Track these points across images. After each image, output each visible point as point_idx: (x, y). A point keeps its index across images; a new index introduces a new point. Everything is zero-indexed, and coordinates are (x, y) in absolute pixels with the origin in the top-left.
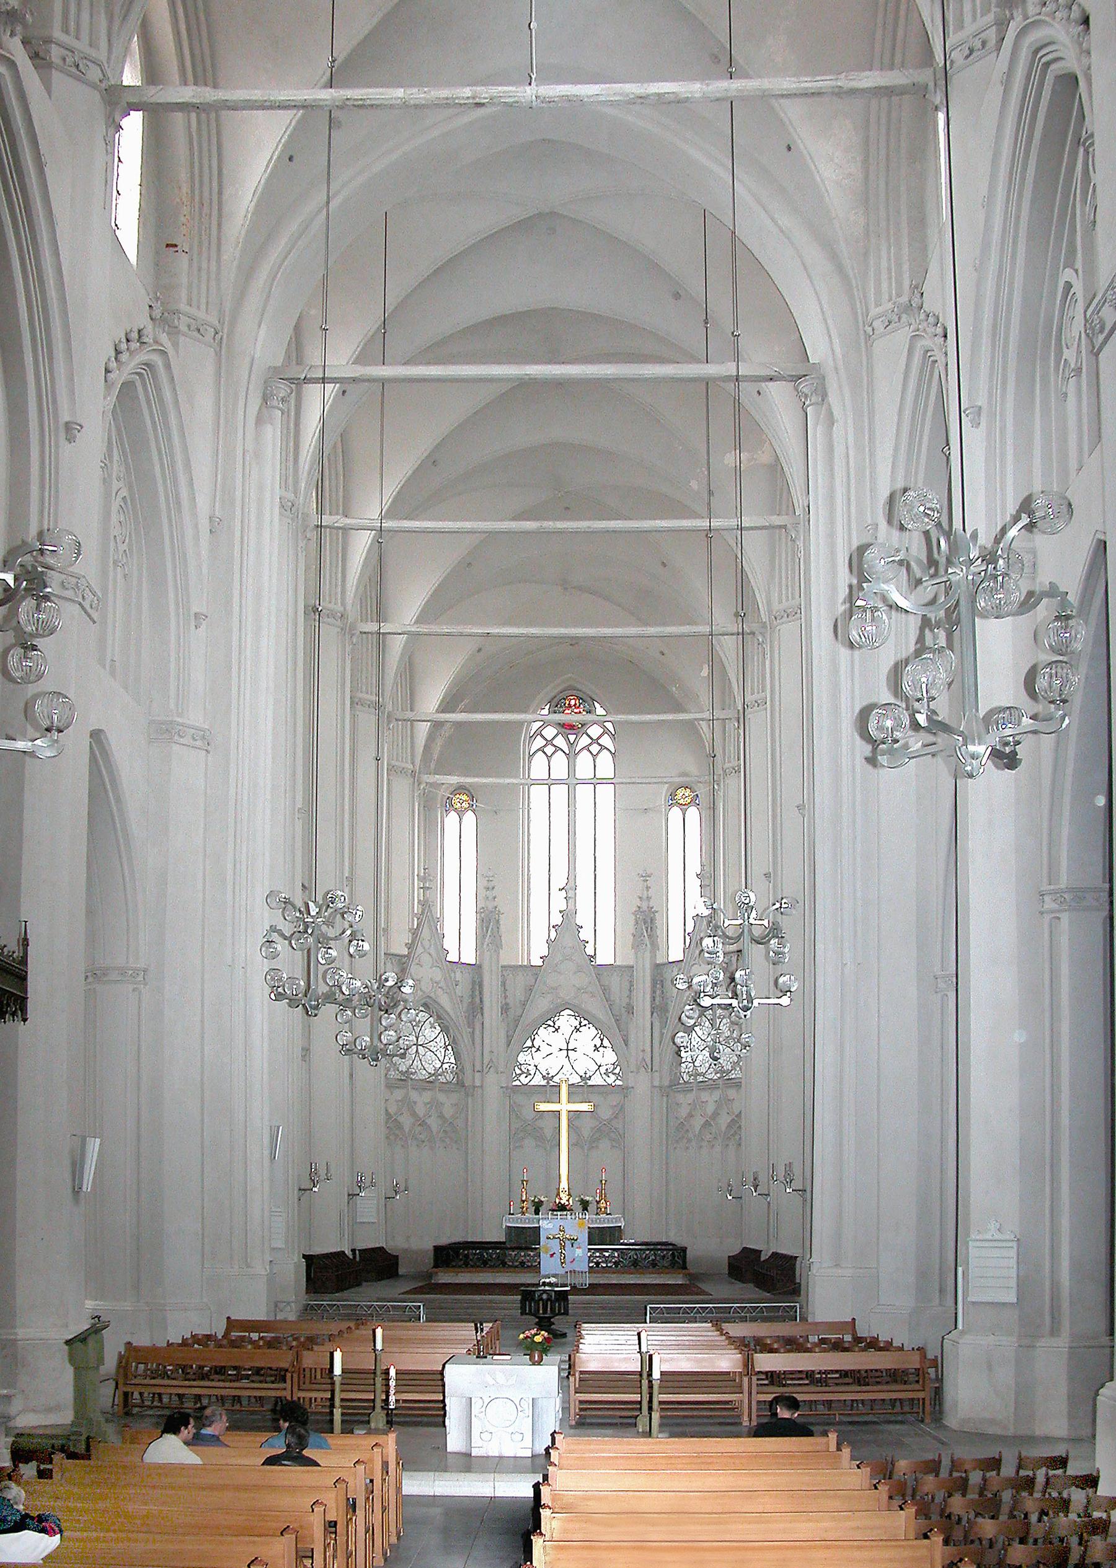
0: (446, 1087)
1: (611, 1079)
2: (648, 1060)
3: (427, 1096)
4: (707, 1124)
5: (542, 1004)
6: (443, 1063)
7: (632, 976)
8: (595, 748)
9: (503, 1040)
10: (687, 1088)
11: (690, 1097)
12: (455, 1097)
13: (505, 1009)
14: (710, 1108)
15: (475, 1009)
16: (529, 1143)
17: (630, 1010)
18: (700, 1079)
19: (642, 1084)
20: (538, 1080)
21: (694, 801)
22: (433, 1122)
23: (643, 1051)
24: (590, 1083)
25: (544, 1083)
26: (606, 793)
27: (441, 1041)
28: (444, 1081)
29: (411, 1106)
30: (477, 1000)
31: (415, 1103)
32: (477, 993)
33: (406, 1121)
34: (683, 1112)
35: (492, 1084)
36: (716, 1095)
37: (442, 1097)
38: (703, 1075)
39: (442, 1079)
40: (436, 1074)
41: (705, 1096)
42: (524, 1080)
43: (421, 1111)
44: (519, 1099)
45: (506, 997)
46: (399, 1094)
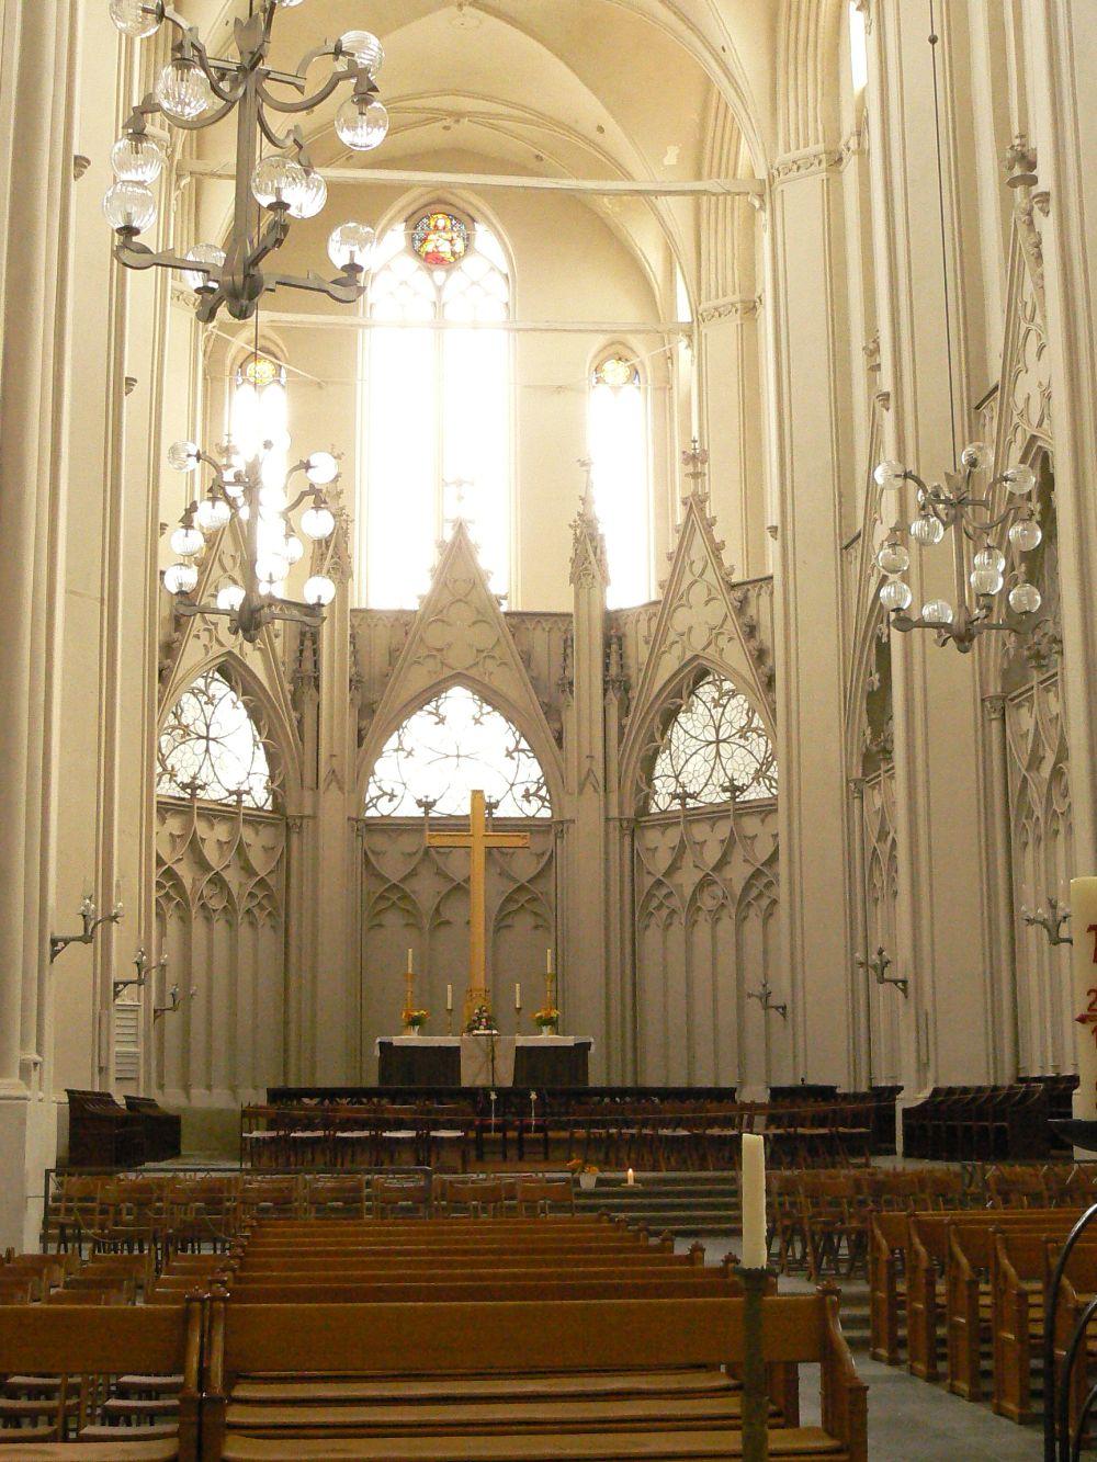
0: (255, 819)
2: (600, 774)
3: (221, 831)
4: (705, 883)
5: (418, 679)
10: (666, 821)
11: (673, 835)
13: (356, 683)
14: (712, 854)
15: (306, 679)
16: (393, 920)
17: (567, 686)
18: (691, 803)
19: (589, 813)
20: (410, 810)
22: (233, 878)
23: (591, 757)
24: (498, 813)
27: (248, 727)
28: (252, 805)
29: (195, 845)
30: (308, 665)
31: (203, 840)
32: (308, 653)
33: (185, 872)
34: (662, 861)
35: (332, 809)
36: (724, 828)
37: (247, 834)
39: (248, 801)
41: (700, 832)
42: (384, 808)
43: (211, 853)
44: (379, 842)
45: (355, 663)
46: (174, 825)
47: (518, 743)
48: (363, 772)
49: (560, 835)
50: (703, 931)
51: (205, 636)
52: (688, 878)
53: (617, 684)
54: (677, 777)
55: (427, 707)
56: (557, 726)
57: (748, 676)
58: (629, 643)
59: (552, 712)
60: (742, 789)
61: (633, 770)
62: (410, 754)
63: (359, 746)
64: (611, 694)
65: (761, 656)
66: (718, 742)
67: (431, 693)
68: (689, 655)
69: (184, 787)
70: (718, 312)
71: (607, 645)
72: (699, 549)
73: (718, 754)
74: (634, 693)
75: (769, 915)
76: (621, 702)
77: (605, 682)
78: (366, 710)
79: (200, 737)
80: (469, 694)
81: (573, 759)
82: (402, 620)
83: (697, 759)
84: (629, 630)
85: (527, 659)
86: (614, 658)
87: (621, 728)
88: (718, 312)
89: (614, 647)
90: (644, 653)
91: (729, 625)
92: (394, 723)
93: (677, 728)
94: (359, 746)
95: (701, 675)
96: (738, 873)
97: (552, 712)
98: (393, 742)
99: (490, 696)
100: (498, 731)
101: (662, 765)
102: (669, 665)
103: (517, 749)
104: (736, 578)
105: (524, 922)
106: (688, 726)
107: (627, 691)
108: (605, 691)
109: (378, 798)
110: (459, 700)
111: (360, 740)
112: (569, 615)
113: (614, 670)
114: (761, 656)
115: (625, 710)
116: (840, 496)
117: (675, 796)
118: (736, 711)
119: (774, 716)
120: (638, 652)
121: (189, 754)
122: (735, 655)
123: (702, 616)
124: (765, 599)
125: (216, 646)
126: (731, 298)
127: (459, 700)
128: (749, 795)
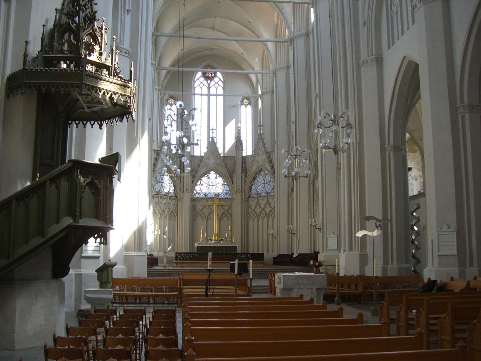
0: (171, 198)
1: (226, 196)
3: (165, 201)
6: (170, 189)
7: (234, 160)
8: (216, 85)
9: (190, 182)
12: (173, 202)
14: (263, 206)
17: (234, 171)
19: (238, 197)
21: (250, 103)
24: (220, 197)
25: (204, 197)
26: (221, 99)
37: (170, 201)
38: (260, 194)
40: (168, 193)
47: (224, 183)
48: (193, 189)
49: (233, 201)
50: (261, 221)
51: (161, 162)
52: (258, 210)
53: (245, 171)
54: (256, 190)
55: (206, 176)
56: (232, 180)
57: (270, 170)
58: (247, 162)
59: (231, 177)
60: (269, 193)
61: (247, 189)
62: (202, 185)
63: (192, 183)
64: (243, 173)
65: (272, 167)
66: (264, 183)
67: (207, 173)
68: (259, 165)
69: (157, 192)
70: (266, 93)
71: (242, 163)
72: (261, 144)
73: (264, 186)
74: (248, 174)
75: (273, 218)
76: (245, 176)
77: (242, 171)
78: (193, 177)
79: (160, 182)
80: (214, 173)
81: (235, 186)
82: (201, 157)
83: (260, 186)
84: (247, 160)
85: (226, 166)
86: (244, 166)
87: (245, 180)
88: (266, 93)
89: (244, 164)
90: (250, 166)
91: (266, 160)
92: (200, 179)
93: (256, 180)
94: (192, 183)
95: (261, 170)
96: (268, 209)
97: (231, 177)
98: (199, 183)
99: (219, 173)
100: (220, 180)
101: (253, 188)
102: (255, 168)
103: (224, 184)
104: (268, 151)
105: (225, 218)
106: (259, 180)
107: (246, 173)
108: (242, 173)
109: (196, 194)
110: (212, 174)
111: (192, 182)
112: (235, 157)
113: (244, 168)
114: (272, 167)
115: (246, 177)
116: (288, 135)
117: (256, 194)
118: (268, 178)
119: (275, 178)
120: (249, 164)
121: (158, 186)
122: (268, 166)
123: (262, 158)
124: (274, 155)
125: (164, 164)
126: (269, 90)
127: (212, 174)
128: (270, 194)
